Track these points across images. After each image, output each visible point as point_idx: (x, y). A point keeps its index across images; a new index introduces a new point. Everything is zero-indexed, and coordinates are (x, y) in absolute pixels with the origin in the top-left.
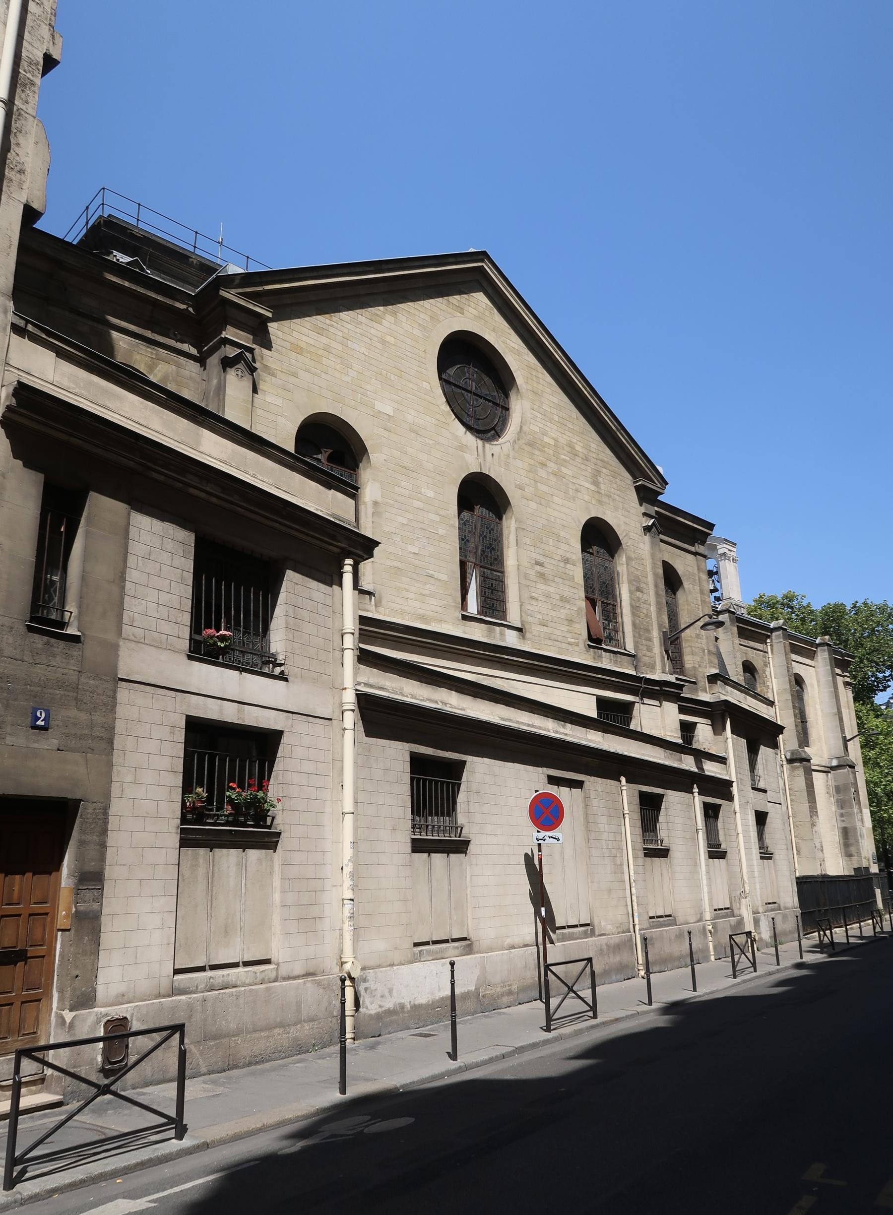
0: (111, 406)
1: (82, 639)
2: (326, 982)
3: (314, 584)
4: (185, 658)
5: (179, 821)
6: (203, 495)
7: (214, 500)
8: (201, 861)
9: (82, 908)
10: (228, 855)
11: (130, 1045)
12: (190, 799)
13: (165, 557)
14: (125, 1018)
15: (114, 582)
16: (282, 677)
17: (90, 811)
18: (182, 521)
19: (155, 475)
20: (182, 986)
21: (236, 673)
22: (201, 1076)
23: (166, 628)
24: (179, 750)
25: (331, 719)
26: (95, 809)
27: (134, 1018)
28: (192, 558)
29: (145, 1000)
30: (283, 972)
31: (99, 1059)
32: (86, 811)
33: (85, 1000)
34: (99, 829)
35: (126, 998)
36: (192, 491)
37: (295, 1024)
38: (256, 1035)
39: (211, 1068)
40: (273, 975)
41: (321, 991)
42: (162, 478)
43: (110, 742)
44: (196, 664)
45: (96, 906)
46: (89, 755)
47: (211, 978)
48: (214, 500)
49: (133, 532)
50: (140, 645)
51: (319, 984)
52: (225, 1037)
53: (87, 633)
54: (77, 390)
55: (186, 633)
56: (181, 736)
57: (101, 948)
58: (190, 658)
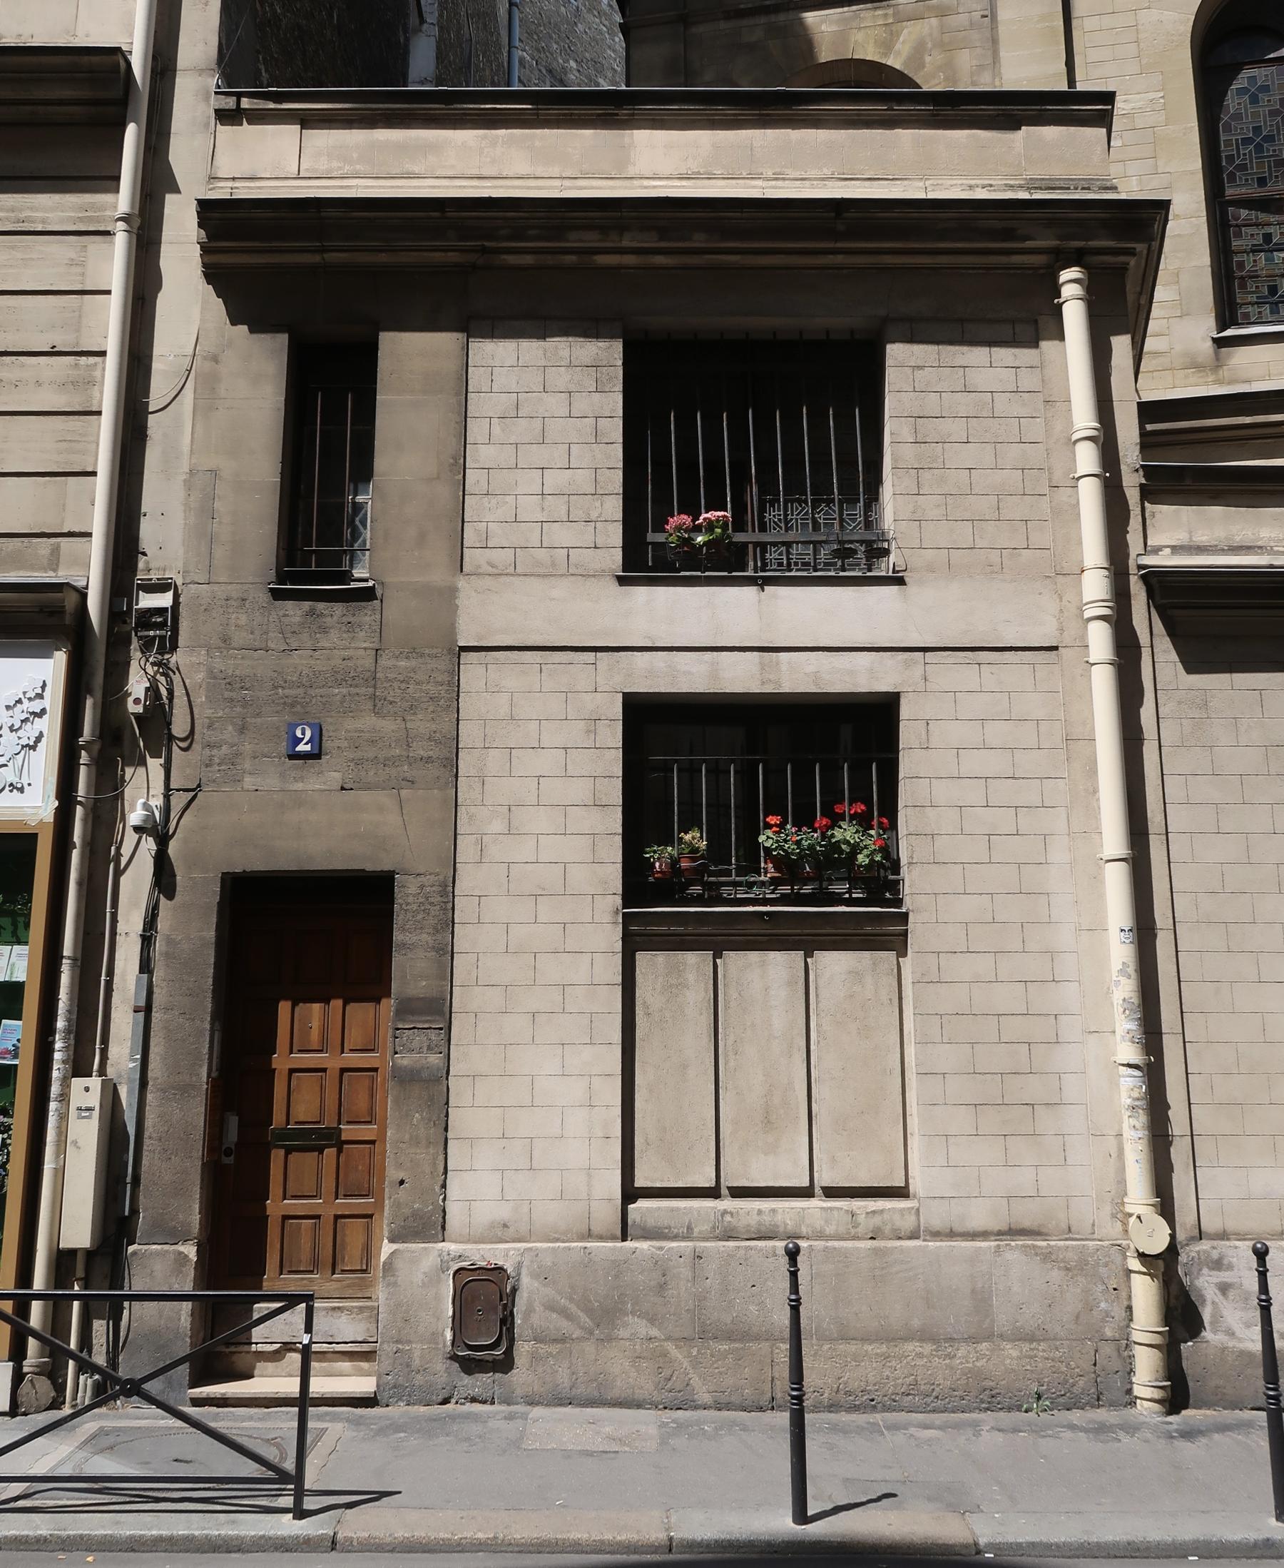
0: (416, 169)
1: (379, 592)
2: (1070, 1255)
3: (977, 355)
4: (614, 586)
5: (619, 900)
6: (630, 260)
7: (660, 260)
8: (691, 977)
9: (405, 1062)
10: (763, 964)
11: (518, 1321)
12: (660, 857)
13: (556, 404)
14: (500, 1269)
15: (438, 478)
16: (897, 580)
17: (413, 889)
18: (589, 327)
19: (512, 259)
20: (651, 1222)
21: (750, 592)
22: (696, 1408)
23: (562, 535)
24: (614, 763)
25: (1056, 648)
26: (422, 887)
27: (524, 1272)
28: (620, 387)
29: (557, 1240)
30: (935, 1217)
31: (449, 1335)
32: (407, 893)
33: (431, 1225)
34: (431, 921)
35: (512, 1230)
36: (602, 260)
37: (974, 1339)
38: (853, 1348)
39: (723, 1399)
40: (908, 1223)
41: (1056, 1275)
42: (528, 260)
43: (452, 764)
44: (641, 592)
45: (435, 1059)
46: (403, 792)
47: (725, 1212)
48: (660, 260)
49: (477, 377)
50: (503, 579)
51: (1047, 1257)
52: (757, 1338)
53: (387, 580)
54: (347, 169)
55: (614, 535)
56: (613, 736)
57: (450, 1135)
58: (622, 581)
